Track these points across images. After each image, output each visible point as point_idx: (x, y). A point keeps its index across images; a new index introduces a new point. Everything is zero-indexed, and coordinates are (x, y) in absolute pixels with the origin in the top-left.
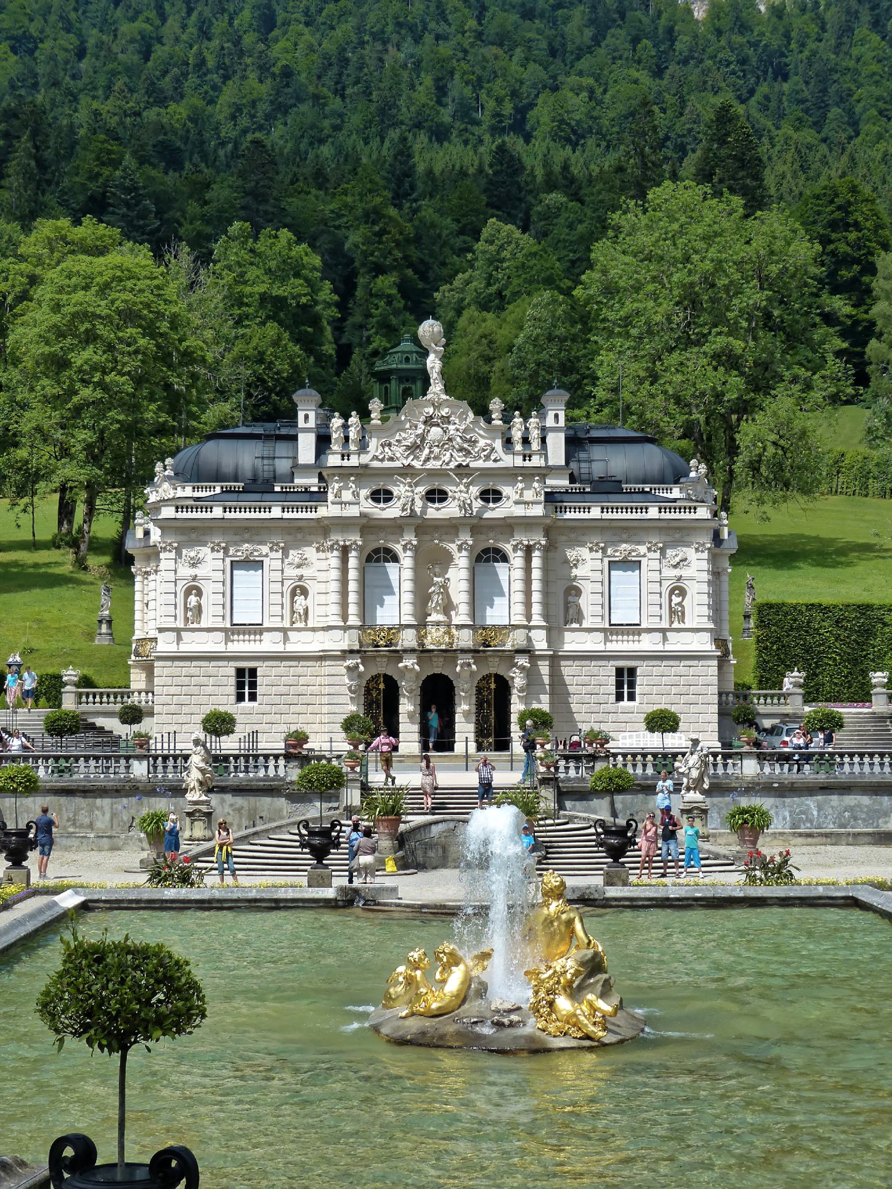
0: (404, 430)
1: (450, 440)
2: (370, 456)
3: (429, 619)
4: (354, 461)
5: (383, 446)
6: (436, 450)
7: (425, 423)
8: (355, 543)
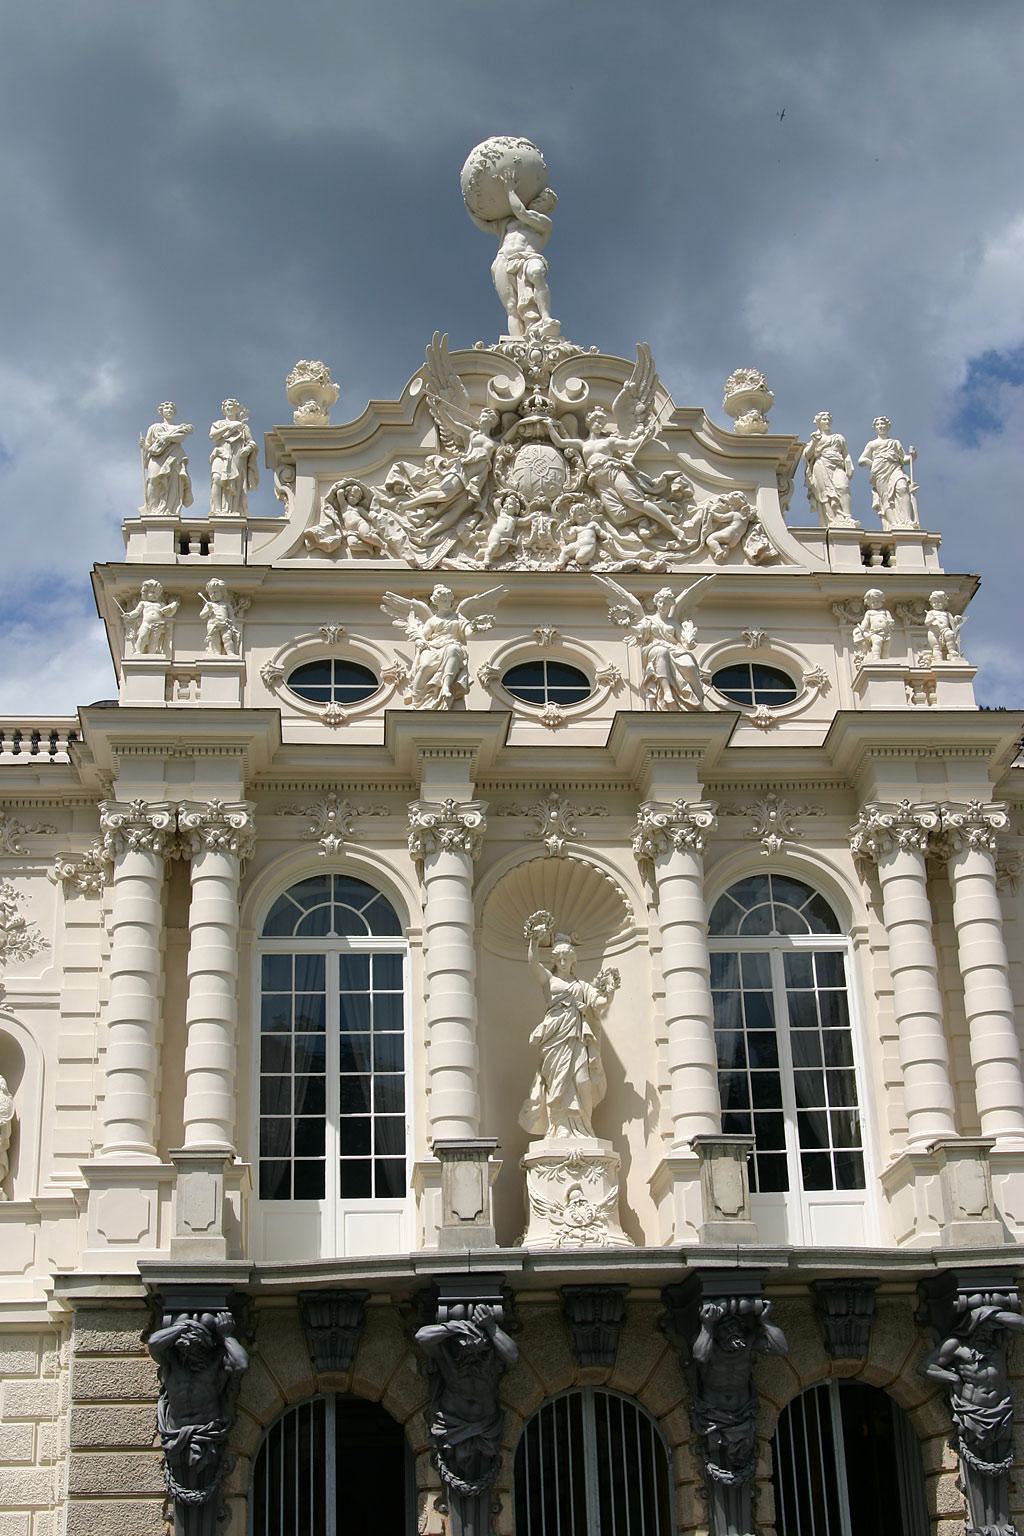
0: (420, 458)
1: (590, 488)
2: (289, 537)
3: (536, 1150)
4: (226, 550)
5: (337, 504)
6: (540, 521)
7: (496, 432)
8: (219, 819)
